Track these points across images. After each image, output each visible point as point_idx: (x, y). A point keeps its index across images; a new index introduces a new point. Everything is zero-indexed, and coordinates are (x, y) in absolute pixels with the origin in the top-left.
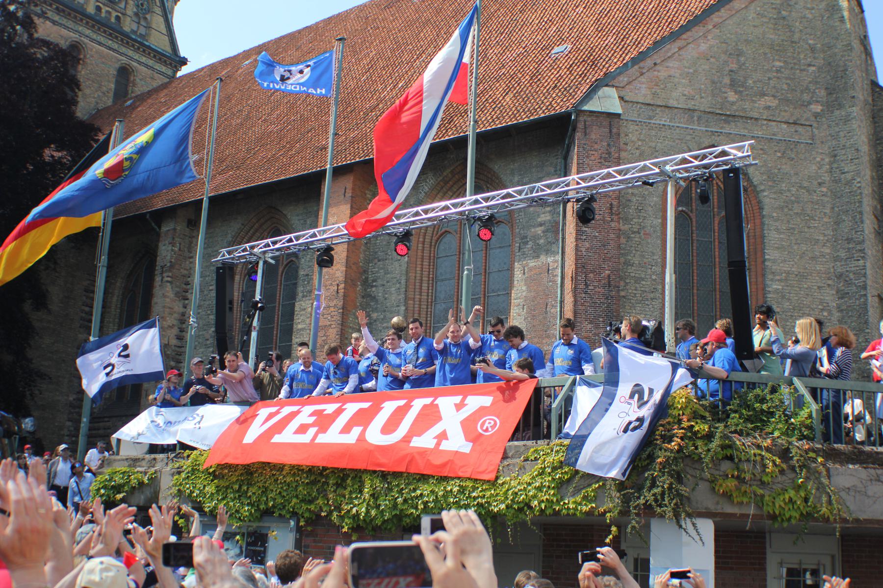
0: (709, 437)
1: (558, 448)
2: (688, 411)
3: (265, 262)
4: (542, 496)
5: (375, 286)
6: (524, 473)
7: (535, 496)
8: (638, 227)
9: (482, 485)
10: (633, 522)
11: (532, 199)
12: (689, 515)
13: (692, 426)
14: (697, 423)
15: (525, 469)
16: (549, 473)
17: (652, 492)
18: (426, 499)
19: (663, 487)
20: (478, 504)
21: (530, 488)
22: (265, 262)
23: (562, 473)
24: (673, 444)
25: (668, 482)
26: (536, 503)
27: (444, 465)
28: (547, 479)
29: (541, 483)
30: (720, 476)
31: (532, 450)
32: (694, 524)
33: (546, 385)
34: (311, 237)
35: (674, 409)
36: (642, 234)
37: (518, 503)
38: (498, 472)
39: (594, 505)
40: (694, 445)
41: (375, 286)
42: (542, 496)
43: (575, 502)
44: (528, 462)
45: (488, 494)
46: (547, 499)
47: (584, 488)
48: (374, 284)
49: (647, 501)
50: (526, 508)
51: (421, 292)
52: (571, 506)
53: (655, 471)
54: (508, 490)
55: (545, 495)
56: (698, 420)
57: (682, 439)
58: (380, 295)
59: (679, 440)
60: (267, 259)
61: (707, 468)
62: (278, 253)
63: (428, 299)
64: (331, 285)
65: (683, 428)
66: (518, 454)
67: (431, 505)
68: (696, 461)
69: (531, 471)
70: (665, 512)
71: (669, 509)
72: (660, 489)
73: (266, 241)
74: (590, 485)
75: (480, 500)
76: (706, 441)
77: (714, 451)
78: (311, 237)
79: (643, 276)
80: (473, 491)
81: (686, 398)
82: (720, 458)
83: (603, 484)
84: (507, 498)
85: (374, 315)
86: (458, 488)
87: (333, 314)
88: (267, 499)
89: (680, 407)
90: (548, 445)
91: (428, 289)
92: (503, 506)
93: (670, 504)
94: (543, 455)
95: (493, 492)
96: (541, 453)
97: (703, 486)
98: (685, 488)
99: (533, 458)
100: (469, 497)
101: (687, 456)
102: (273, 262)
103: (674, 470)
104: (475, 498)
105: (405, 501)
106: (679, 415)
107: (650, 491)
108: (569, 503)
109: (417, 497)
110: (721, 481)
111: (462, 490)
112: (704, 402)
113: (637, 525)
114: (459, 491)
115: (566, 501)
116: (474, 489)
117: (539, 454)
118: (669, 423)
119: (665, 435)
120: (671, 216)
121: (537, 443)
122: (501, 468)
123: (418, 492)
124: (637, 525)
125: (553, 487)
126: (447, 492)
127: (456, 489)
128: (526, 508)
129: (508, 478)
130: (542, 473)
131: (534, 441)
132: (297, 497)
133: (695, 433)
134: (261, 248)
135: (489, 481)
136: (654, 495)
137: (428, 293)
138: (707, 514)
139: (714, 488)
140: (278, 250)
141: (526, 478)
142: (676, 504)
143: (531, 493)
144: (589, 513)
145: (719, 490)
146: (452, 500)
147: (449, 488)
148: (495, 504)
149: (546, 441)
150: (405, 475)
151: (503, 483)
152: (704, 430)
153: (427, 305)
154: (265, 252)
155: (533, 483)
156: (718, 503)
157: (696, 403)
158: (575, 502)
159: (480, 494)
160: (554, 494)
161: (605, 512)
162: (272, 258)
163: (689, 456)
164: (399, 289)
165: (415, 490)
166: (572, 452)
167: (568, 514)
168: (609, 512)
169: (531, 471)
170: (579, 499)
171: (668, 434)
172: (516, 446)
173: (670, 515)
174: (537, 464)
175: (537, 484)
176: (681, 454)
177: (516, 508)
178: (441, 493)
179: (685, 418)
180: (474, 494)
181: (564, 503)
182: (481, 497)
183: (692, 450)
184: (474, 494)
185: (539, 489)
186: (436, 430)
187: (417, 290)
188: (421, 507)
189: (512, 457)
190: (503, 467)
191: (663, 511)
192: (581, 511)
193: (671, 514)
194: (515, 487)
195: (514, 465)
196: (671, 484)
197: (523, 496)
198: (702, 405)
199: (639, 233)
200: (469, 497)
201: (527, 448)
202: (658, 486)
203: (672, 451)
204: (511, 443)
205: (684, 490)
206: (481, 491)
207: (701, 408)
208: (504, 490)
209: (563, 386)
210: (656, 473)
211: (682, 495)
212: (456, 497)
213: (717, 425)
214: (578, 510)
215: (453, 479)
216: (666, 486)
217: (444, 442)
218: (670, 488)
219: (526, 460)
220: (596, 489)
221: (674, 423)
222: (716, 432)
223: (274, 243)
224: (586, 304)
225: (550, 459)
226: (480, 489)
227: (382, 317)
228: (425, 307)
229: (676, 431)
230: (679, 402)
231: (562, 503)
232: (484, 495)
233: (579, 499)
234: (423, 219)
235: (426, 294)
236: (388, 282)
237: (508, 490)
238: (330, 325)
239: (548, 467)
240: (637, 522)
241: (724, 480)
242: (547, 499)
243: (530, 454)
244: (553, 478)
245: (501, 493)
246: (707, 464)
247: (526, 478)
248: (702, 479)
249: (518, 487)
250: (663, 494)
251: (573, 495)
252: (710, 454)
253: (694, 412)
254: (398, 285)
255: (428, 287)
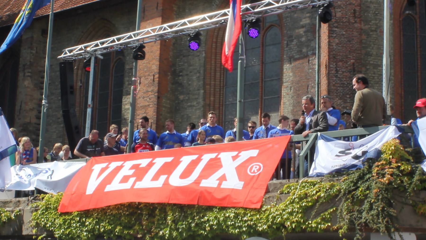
0: (411, 174)
1: (304, 184)
2: (396, 156)
3: (96, 58)
4: (293, 218)
5: (181, 76)
6: (280, 203)
7: (288, 219)
8: (375, 27)
9: (250, 212)
10: (358, 235)
11: (287, 7)
12: (397, 230)
13: (398, 167)
14: (402, 164)
15: (281, 200)
16: (298, 202)
17: (370, 214)
18: (211, 223)
19: (377, 209)
20: (248, 224)
21: (284, 213)
22: (96, 58)
23: (307, 202)
24: (385, 179)
25: (381, 206)
26: (289, 223)
27: (224, 199)
28: (296, 206)
29: (292, 209)
30: (420, 202)
31: (286, 186)
32: (401, 236)
33: (296, 140)
34: (129, 38)
35: (387, 154)
36: (378, 32)
37: (276, 224)
38: (262, 202)
39: (330, 224)
40: (400, 180)
41: (181, 76)
42: (293, 218)
43: (315, 223)
44: (283, 195)
45: (255, 218)
46: (296, 220)
47: (323, 212)
48: (181, 74)
49: (367, 220)
50: (281, 227)
51: (215, 79)
52: (314, 225)
53: (372, 198)
54: (269, 215)
55: (295, 217)
56: (403, 162)
57: (392, 175)
58: (185, 82)
59: (389, 176)
60: (97, 55)
61: (410, 196)
62: (105, 51)
63: (220, 84)
64: (149, 75)
65: (392, 168)
66: (276, 189)
67: (215, 227)
68: (403, 191)
69: (285, 201)
70: (379, 228)
71: (383, 225)
72: (376, 211)
73: (96, 42)
74: (326, 210)
75: (249, 222)
76: (409, 177)
77: (415, 184)
78: (129, 38)
79: (379, 63)
80: (244, 216)
81: (395, 146)
82: (420, 189)
83: (336, 209)
84: (268, 221)
85: (181, 97)
86: (233, 214)
87: (150, 97)
88: (99, 227)
89: (390, 152)
90: (297, 182)
91: (221, 77)
92: (265, 227)
93: (383, 222)
94: (294, 189)
95: (258, 216)
96: (292, 188)
97: (407, 210)
98: (393, 210)
99: (286, 192)
100: (242, 220)
101: (395, 188)
102: (101, 57)
103: (386, 198)
104: (246, 221)
105: (197, 225)
106: (390, 158)
107: (369, 213)
108: (312, 223)
109: (205, 222)
110: (420, 205)
111: (237, 216)
112: (408, 149)
113: (360, 238)
114: (234, 216)
115: (310, 222)
116: (245, 214)
117: (291, 189)
118: (382, 164)
119: (379, 173)
120: (387, 16)
121: (289, 181)
122: (264, 200)
123: (206, 218)
124: (360, 238)
125: (301, 212)
126: (226, 217)
127: (232, 215)
128: (281, 227)
129: (269, 207)
130: (292, 202)
131: (287, 180)
132: (120, 225)
133: (402, 171)
134: (93, 47)
135: (255, 209)
136: (372, 215)
137: (220, 79)
138: (410, 230)
139: (415, 211)
140: (105, 48)
141: (282, 206)
142: (387, 222)
143: (285, 217)
144: (327, 230)
145: (419, 212)
146: (229, 223)
147: (227, 215)
148: (260, 225)
149: (296, 180)
150: (197, 206)
151: (266, 210)
152: (408, 169)
153: (220, 89)
154: (95, 51)
155: (286, 209)
156: (418, 222)
157: (402, 150)
158: (315, 223)
159: (249, 218)
160: (301, 216)
161: (338, 229)
162: (102, 55)
163: (397, 188)
164: (199, 77)
165: (203, 217)
166: (314, 187)
167: (311, 231)
168: (341, 228)
169: (285, 201)
170: (319, 220)
171: (382, 172)
172: (275, 184)
173: (383, 229)
174: (289, 196)
175: (290, 210)
176: (390, 186)
177: (275, 227)
178: (222, 219)
179: (394, 161)
180: (245, 219)
181: (309, 223)
182: (250, 220)
183: (399, 183)
184: (245, 219)
185: (291, 214)
186: (218, 174)
187: (213, 78)
188: (208, 229)
189: (273, 191)
190: (266, 199)
191: (378, 227)
192: (321, 228)
193: (384, 229)
194: (274, 213)
195: (273, 197)
196: (383, 208)
197: (279, 219)
198: (408, 152)
199: (376, 31)
200: (242, 220)
201: (282, 185)
202: (374, 210)
203: (384, 184)
204: (271, 182)
205: (393, 211)
206: (250, 216)
207: (406, 154)
208: (266, 215)
209: (309, 140)
210: (373, 200)
211: (392, 215)
212: (232, 221)
213: (417, 166)
214: (318, 227)
215: (230, 208)
216: (379, 209)
217: (224, 182)
218: (383, 210)
219: (282, 193)
220: (331, 212)
221: (386, 164)
222: (416, 170)
223: (102, 43)
224: (336, 85)
225: (298, 192)
226: (249, 215)
227: (187, 98)
228: (218, 90)
229: (387, 170)
230: (389, 149)
231: (307, 224)
232: (252, 219)
233: (319, 220)
234: (209, 23)
235: (219, 81)
236: (191, 72)
237: (269, 215)
238: (149, 105)
239: (297, 197)
240: (360, 235)
241: (423, 204)
242: (296, 220)
243: (284, 189)
244: (300, 206)
245: (264, 217)
246: (410, 193)
247: (282, 206)
248: (407, 204)
249: (276, 213)
250: (378, 215)
251: (316, 217)
252: (412, 186)
253: (401, 157)
254: (198, 75)
255: (221, 75)
